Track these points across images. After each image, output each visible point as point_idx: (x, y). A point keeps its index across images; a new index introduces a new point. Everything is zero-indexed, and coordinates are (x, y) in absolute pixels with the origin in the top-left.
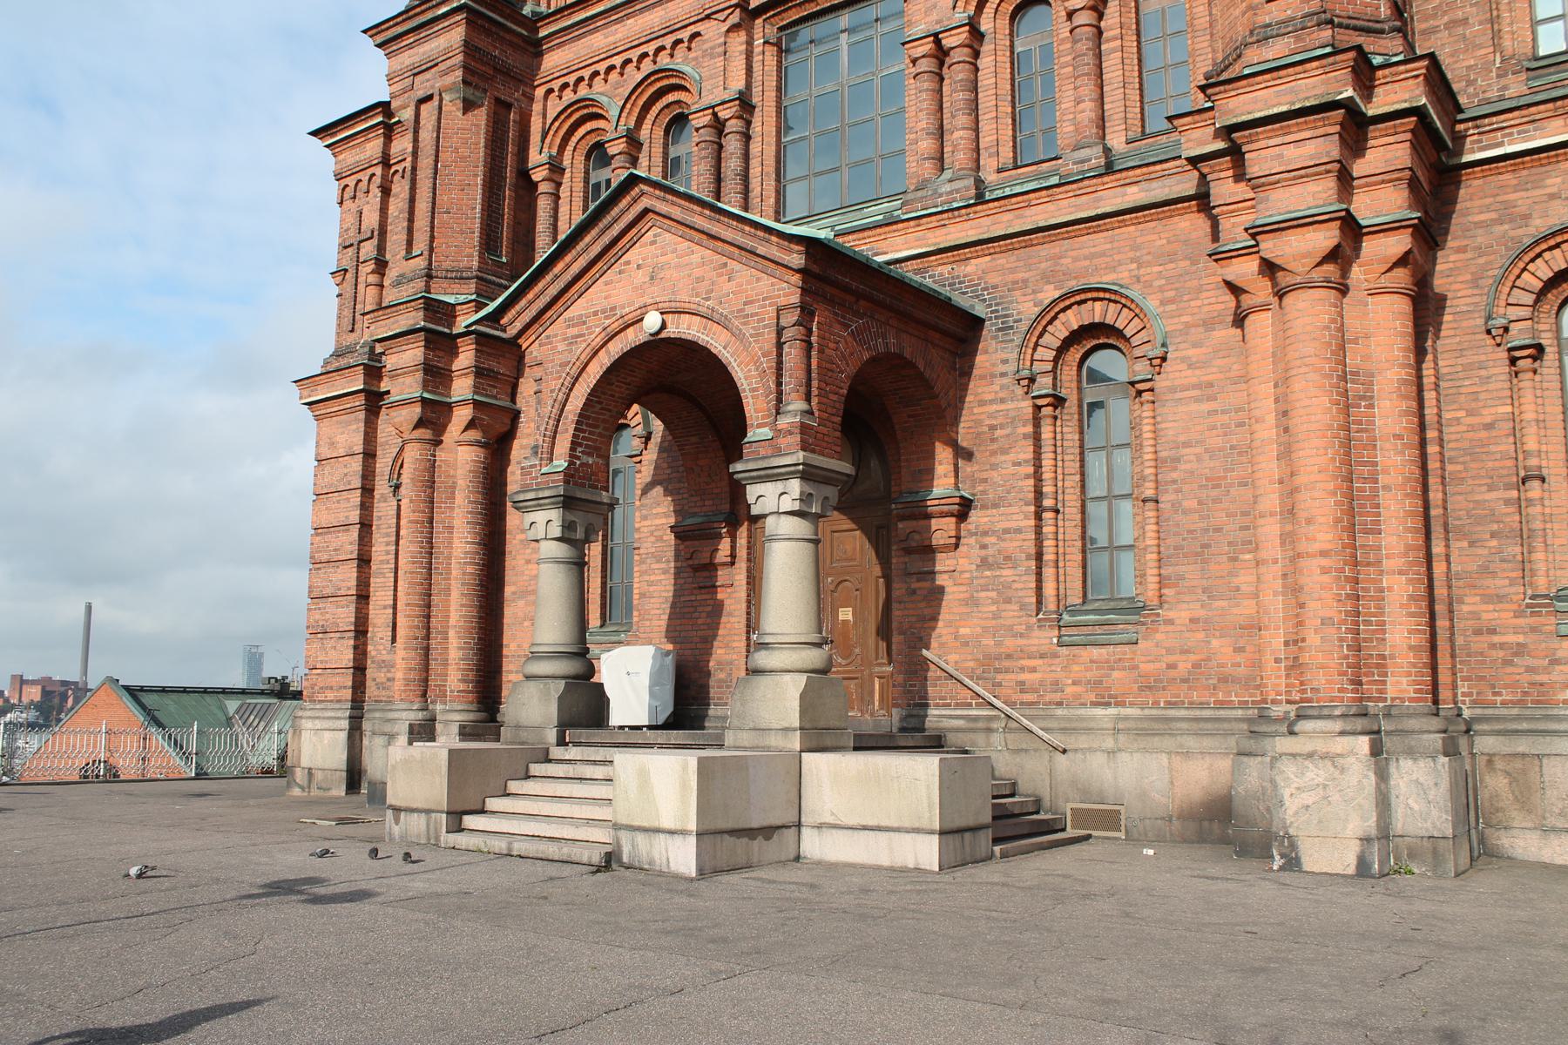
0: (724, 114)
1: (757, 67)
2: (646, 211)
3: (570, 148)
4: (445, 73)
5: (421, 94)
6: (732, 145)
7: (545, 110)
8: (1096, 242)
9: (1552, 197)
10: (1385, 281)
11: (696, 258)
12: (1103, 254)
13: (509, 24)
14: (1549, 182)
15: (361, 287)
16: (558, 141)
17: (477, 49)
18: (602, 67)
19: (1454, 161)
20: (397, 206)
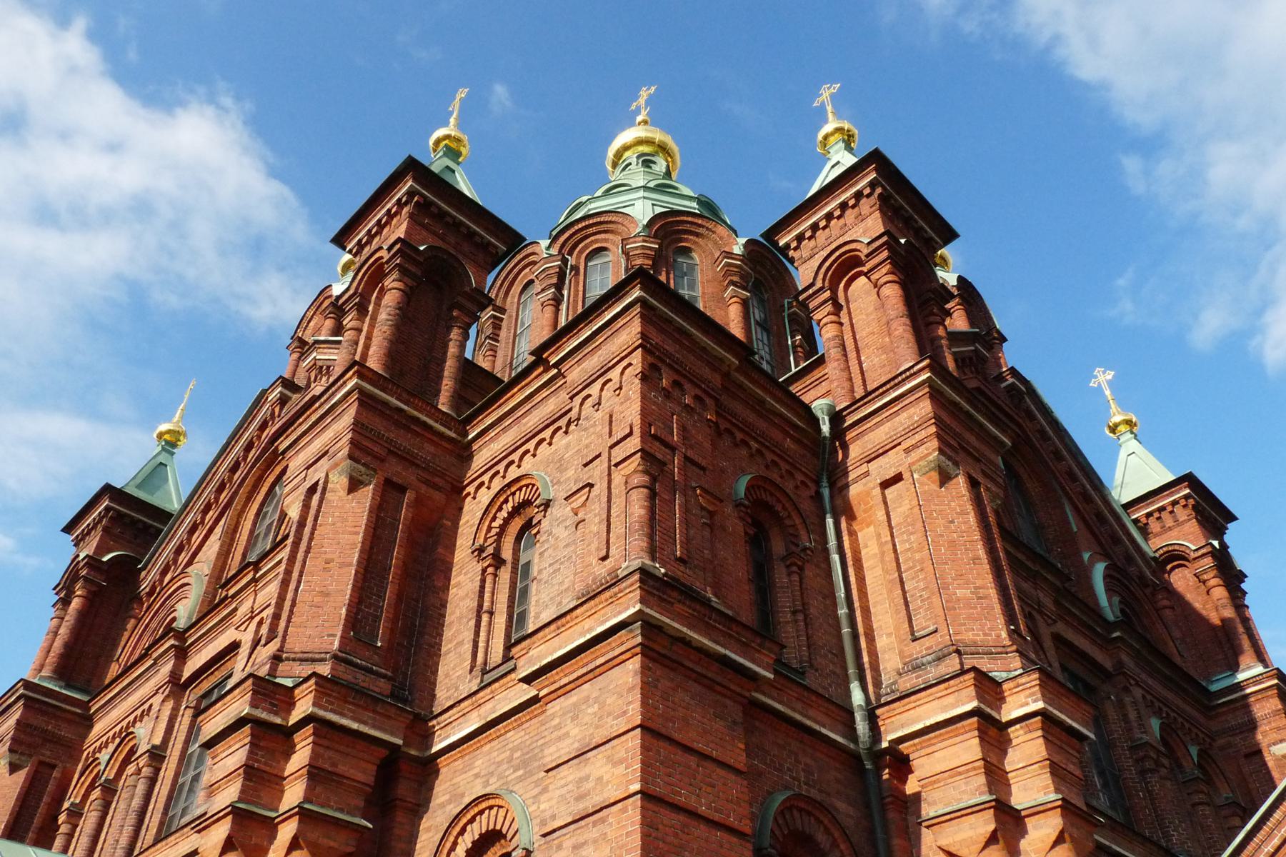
9: (477, 776)
13: (64, 706)
14: (479, 763)
16: (83, 791)
17: (29, 726)
19: (427, 754)
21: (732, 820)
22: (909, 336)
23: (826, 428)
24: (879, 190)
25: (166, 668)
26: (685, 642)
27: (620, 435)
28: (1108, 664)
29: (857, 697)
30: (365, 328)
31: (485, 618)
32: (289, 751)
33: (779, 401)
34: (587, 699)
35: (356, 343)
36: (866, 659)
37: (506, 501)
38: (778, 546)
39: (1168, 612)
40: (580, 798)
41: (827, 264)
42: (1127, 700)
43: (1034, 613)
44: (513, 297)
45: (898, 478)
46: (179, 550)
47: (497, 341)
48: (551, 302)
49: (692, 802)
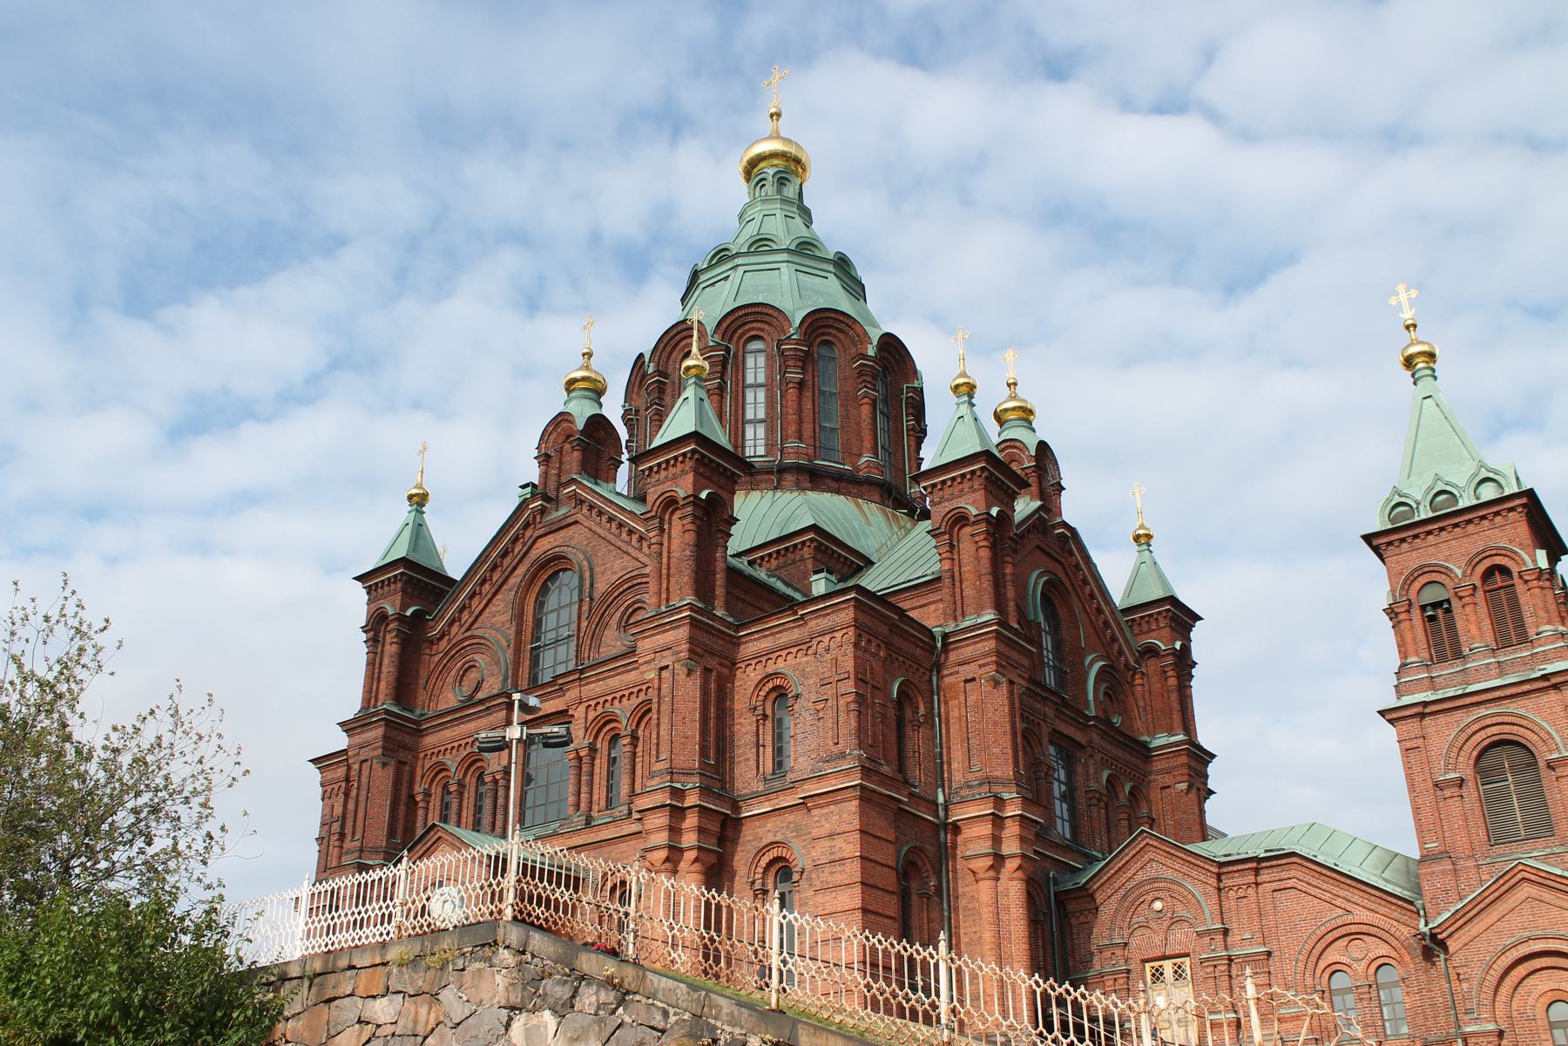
0: (498, 777)
2: (440, 838)
3: (435, 784)
4: (374, 749)
5: (363, 758)
12: (625, 852)
15: (331, 848)
17: (389, 738)
20: (351, 806)
23: (939, 645)
24: (986, 474)
26: (874, 791)
27: (842, 676)
28: (1084, 742)
29: (941, 799)
30: (666, 544)
31: (761, 749)
32: (683, 819)
33: (913, 628)
34: (832, 812)
36: (946, 775)
37: (768, 682)
38: (908, 713)
39: (1139, 688)
40: (831, 854)
41: (949, 516)
42: (1091, 762)
43: (1042, 723)
44: (675, 362)
45: (973, 679)
46: (462, 609)
47: (663, 406)
48: (717, 391)
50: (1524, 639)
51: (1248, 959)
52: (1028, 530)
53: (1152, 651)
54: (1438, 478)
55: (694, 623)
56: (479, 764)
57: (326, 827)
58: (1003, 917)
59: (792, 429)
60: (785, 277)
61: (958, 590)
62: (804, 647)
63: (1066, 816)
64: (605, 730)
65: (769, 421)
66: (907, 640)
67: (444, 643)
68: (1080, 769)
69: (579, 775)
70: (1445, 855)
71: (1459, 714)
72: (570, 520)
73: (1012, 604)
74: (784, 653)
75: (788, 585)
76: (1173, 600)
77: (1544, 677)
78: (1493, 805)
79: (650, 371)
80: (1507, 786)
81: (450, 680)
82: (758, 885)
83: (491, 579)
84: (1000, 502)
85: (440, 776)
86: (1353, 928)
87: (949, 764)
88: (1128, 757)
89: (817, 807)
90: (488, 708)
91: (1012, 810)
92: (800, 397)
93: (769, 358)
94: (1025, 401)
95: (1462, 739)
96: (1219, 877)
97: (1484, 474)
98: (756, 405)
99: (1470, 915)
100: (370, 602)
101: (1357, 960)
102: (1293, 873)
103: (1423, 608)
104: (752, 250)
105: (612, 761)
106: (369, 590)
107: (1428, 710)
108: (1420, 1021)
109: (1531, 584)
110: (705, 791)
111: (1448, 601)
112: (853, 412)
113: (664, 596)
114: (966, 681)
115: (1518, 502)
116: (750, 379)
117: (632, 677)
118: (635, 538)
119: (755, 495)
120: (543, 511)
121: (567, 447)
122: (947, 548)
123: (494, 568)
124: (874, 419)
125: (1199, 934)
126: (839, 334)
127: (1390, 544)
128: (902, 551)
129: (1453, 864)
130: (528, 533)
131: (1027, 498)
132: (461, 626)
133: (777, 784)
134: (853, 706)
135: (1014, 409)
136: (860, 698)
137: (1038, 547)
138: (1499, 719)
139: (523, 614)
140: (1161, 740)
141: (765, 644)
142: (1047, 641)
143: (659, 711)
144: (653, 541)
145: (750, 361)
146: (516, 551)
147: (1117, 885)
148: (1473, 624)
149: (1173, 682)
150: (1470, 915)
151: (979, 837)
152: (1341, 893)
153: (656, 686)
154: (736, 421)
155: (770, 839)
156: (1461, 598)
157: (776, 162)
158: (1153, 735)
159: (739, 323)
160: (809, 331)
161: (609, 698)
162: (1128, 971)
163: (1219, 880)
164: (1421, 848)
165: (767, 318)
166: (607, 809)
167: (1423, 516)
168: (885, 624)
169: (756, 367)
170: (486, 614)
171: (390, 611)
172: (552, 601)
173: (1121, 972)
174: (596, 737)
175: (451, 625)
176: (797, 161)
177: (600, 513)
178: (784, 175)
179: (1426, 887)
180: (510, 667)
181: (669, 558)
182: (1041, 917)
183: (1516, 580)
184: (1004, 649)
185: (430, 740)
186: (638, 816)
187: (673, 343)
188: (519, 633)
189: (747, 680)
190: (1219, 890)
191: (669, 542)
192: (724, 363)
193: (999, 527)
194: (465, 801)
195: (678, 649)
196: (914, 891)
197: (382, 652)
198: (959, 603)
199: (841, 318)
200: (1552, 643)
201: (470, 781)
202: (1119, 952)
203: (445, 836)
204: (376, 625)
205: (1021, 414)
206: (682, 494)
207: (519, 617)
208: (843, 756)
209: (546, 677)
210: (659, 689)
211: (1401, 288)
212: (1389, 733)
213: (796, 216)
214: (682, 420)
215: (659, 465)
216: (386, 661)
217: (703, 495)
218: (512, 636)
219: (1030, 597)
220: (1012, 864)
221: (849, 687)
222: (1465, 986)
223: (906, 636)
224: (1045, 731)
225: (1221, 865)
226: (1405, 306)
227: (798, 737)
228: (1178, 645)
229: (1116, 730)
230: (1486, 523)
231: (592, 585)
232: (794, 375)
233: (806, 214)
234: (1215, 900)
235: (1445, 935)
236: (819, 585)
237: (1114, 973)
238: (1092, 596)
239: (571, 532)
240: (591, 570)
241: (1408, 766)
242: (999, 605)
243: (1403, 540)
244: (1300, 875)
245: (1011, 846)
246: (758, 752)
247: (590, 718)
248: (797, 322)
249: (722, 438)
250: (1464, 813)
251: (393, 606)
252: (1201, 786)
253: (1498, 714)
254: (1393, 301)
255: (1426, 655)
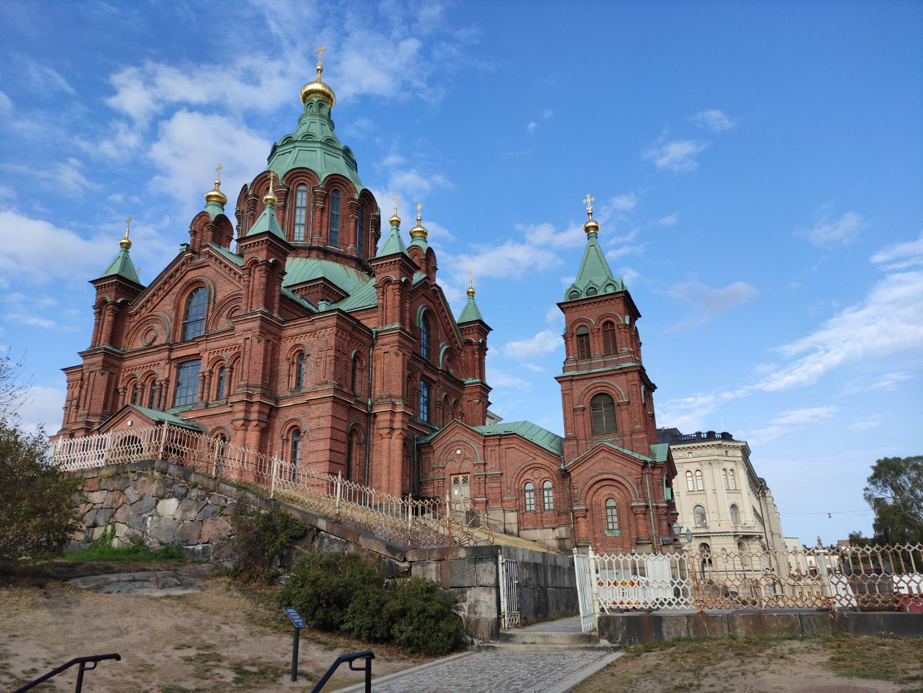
0: (162, 383)
1: (172, 372)
2: (130, 411)
3: (129, 384)
5: (91, 370)
6: (164, 390)
7: (124, 375)
8: (222, 418)
10: (254, 429)
11: (138, 421)
15: (71, 412)
18: (138, 367)
20: (83, 392)
21: (344, 430)
22: (398, 314)
23: (374, 336)
24: (401, 263)
25: (167, 353)
26: (339, 399)
27: (329, 348)
28: (436, 380)
29: (369, 403)
31: (291, 377)
35: (249, 286)
38: (358, 365)
44: (263, 191)
45: (388, 352)
46: (147, 302)
48: (282, 208)
49: (338, 427)
50: (616, 353)
51: (493, 476)
52: (419, 287)
53: (469, 342)
54: (591, 282)
55: (262, 319)
56: (153, 376)
57: (69, 402)
58: (392, 454)
59: (317, 229)
60: (319, 156)
61: (385, 313)
62: (313, 334)
63: (425, 411)
64: (218, 364)
65: (307, 225)
66: (360, 333)
67: (137, 317)
68: (433, 391)
69: (204, 384)
70: (575, 438)
71: (586, 381)
72: (205, 264)
73: (408, 320)
74: (304, 335)
75: (309, 303)
76: (480, 322)
77: (621, 369)
78: (595, 419)
79: (250, 193)
80: (602, 412)
81: (140, 335)
82: (285, 437)
83: (163, 288)
84: (407, 275)
85: (132, 381)
86: (536, 466)
87: (375, 388)
88: (455, 387)
89: (313, 404)
90: (159, 350)
91: (399, 409)
92: (322, 215)
93: (309, 195)
94: (424, 228)
95: (586, 392)
96: (484, 441)
97: (609, 282)
98: (301, 217)
99: (580, 463)
100: (98, 294)
101: (536, 479)
102: (514, 442)
103: (579, 336)
104: (304, 139)
105: (220, 378)
106: (97, 288)
107: (574, 379)
108: (558, 504)
109: (621, 330)
110: (263, 395)
111: (587, 334)
112: (346, 224)
113: (249, 305)
114: (385, 353)
115: (620, 295)
116: (298, 204)
117: (232, 341)
118: (237, 276)
119: (297, 260)
120: (192, 258)
121: (205, 228)
122: (381, 294)
123: (165, 283)
124: (356, 229)
125: (474, 465)
126: (343, 187)
127: (568, 308)
128: (363, 291)
129: (577, 442)
130: (184, 268)
131: (421, 272)
132: (147, 310)
133: (297, 394)
134: (333, 361)
135: (419, 231)
136: (336, 358)
137: (423, 295)
138: (602, 384)
139: (179, 307)
140: (470, 381)
141: (296, 331)
142: (424, 336)
143: (243, 358)
144: (245, 279)
145: (299, 195)
146: (177, 276)
147: (443, 442)
148: (597, 345)
149: (477, 356)
150: (580, 463)
151: (384, 420)
152: (533, 451)
153: (243, 346)
154: (291, 223)
155: (292, 417)
156: (593, 333)
157: (318, 95)
158: (467, 379)
159: (295, 176)
160: (328, 184)
161: (221, 350)
162: (444, 479)
163: (484, 442)
164: (566, 435)
165: (308, 175)
166: (216, 400)
167: (583, 298)
168: (350, 326)
169: (302, 199)
170: (160, 305)
171: (109, 300)
172: (194, 302)
173: (441, 479)
174: (213, 367)
175: (141, 308)
176: (329, 96)
177: (221, 263)
178: (322, 103)
179: (565, 450)
180: (172, 331)
181: (253, 288)
182: (410, 455)
183: (616, 328)
184: (402, 340)
185: (127, 363)
186: (231, 405)
187: (262, 181)
188: (177, 315)
189: (286, 347)
190: (484, 446)
191: (253, 281)
192: (286, 194)
193: (404, 287)
194: (145, 394)
195: (254, 331)
196: (354, 442)
197: (104, 319)
198: (385, 318)
199: (344, 179)
200: (626, 355)
201: (148, 383)
202: (441, 471)
203: (133, 411)
204: (100, 306)
205: (422, 234)
206: (260, 259)
207: (177, 308)
208: (326, 383)
209: (190, 338)
210: (244, 348)
211: (588, 196)
212: (558, 386)
213: (326, 124)
214: (262, 225)
215: (250, 244)
216: (105, 324)
217: (271, 261)
218: (173, 317)
219: (418, 317)
220: (397, 432)
221: (332, 353)
222: (576, 491)
223: (359, 331)
224: (419, 375)
225: (486, 436)
226: (589, 204)
227: (308, 373)
228: (481, 341)
229: (450, 376)
230: (607, 302)
231: (215, 296)
232: (320, 204)
233: (332, 125)
234: (482, 451)
235: (570, 470)
236: (323, 306)
237: (438, 479)
238: (445, 317)
239: (205, 270)
240: (215, 289)
241: (564, 401)
242: (402, 321)
243: (573, 307)
244: (517, 442)
245: (397, 425)
246: (289, 378)
247: (211, 358)
248: (323, 179)
249: (281, 235)
250: (583, 421)
251: (111, 297)
252: (485, 401)
253: (601, 383)
254: (584, 202)
255: (576, 356)
